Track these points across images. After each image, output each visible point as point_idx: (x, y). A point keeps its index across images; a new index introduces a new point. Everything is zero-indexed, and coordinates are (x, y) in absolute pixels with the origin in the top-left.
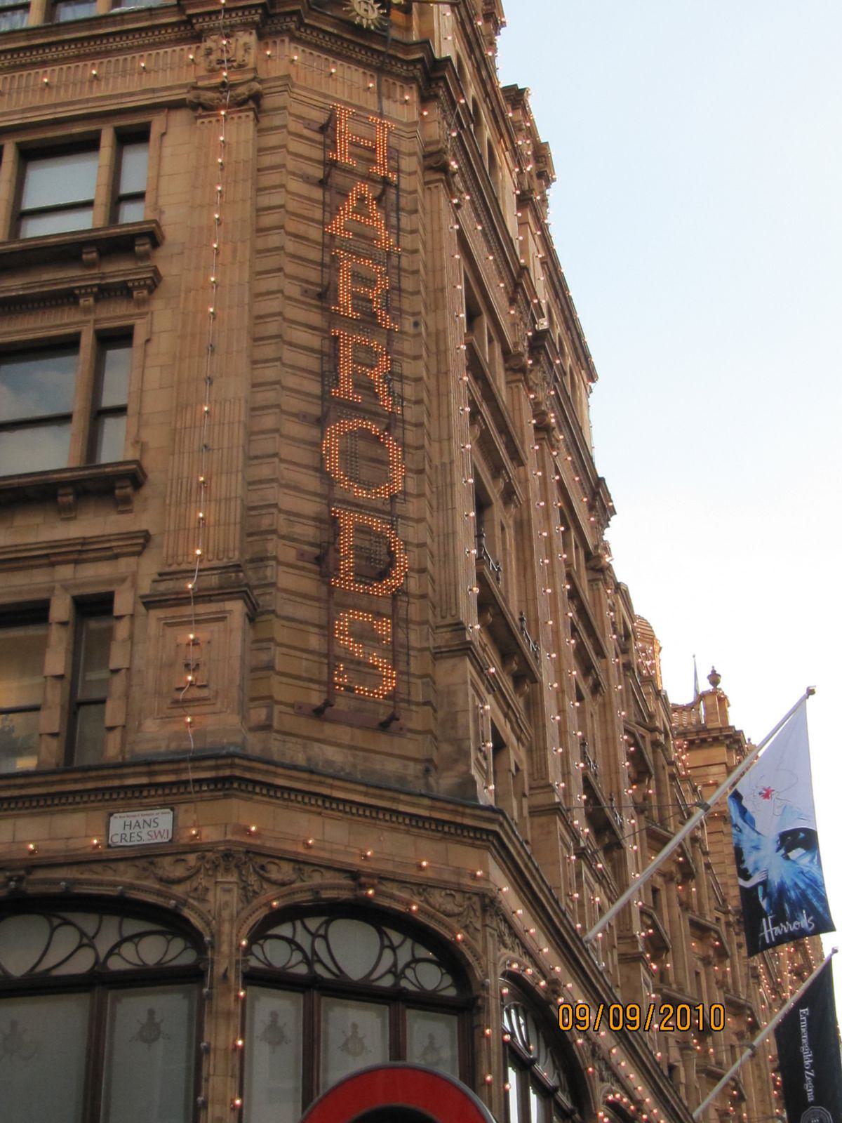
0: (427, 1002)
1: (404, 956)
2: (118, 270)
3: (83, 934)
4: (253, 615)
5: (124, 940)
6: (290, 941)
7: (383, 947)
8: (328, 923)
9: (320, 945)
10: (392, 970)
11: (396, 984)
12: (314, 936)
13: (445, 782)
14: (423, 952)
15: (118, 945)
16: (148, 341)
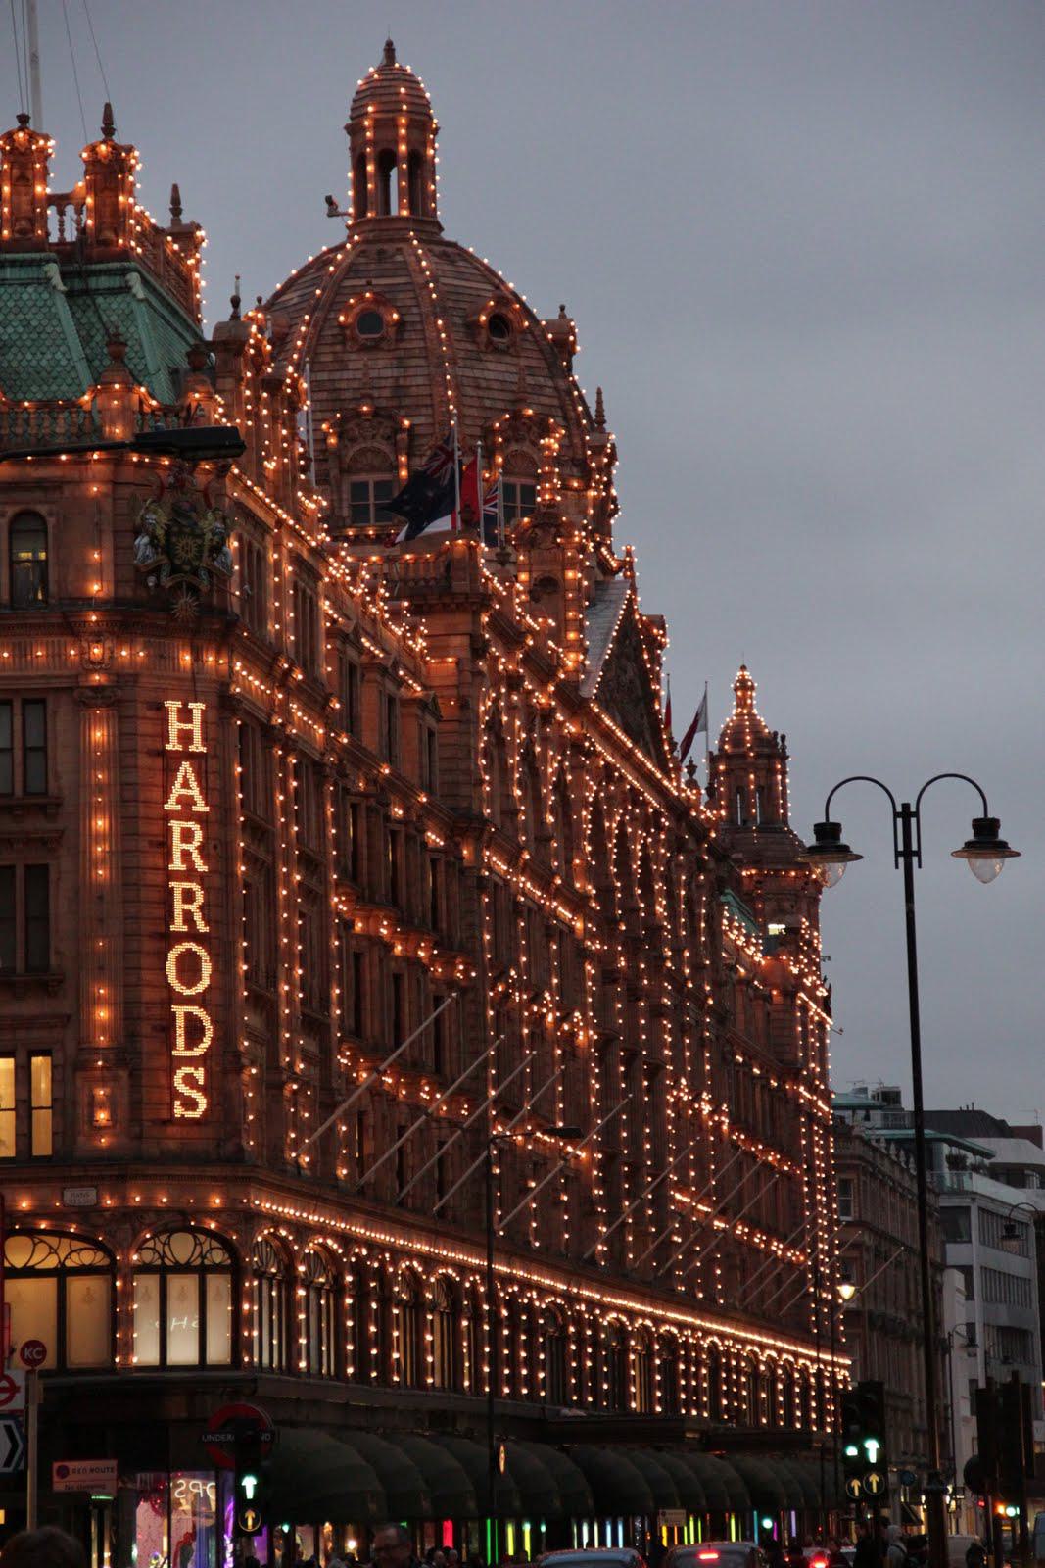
0: (217, 1269)
1: (206, 1247)
2: (36, 825)
3: (51, 1247)
4: (131, 1075)
5: (72, 1252)
6: (153, 1249)
7: (196, 1244)
8: (169, 1237)
9: (166, 1247)
10: (202, 1257)
11: (202, 1262)
12: (164, 1244)
13: (230, 1147)
14: (215, 1243)
15: (69, 1254)
16: (58, 879)
